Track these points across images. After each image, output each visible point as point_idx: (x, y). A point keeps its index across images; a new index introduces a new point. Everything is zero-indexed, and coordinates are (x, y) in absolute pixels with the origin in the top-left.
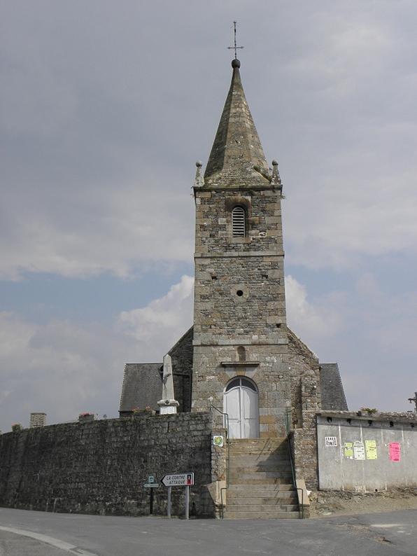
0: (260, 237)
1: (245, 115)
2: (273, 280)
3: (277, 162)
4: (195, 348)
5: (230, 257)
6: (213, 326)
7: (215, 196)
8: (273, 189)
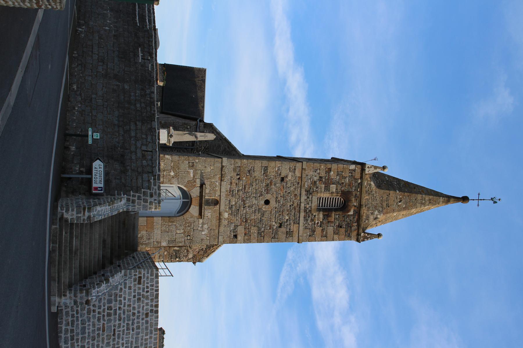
0: (316, 222)
1: (422, 208)
2: (276, 233)
3: (380, 239)
4: (220, 160)
5: (301, 194)
6: (238, 177)
7: (356, 182)
8: (358, 234)
